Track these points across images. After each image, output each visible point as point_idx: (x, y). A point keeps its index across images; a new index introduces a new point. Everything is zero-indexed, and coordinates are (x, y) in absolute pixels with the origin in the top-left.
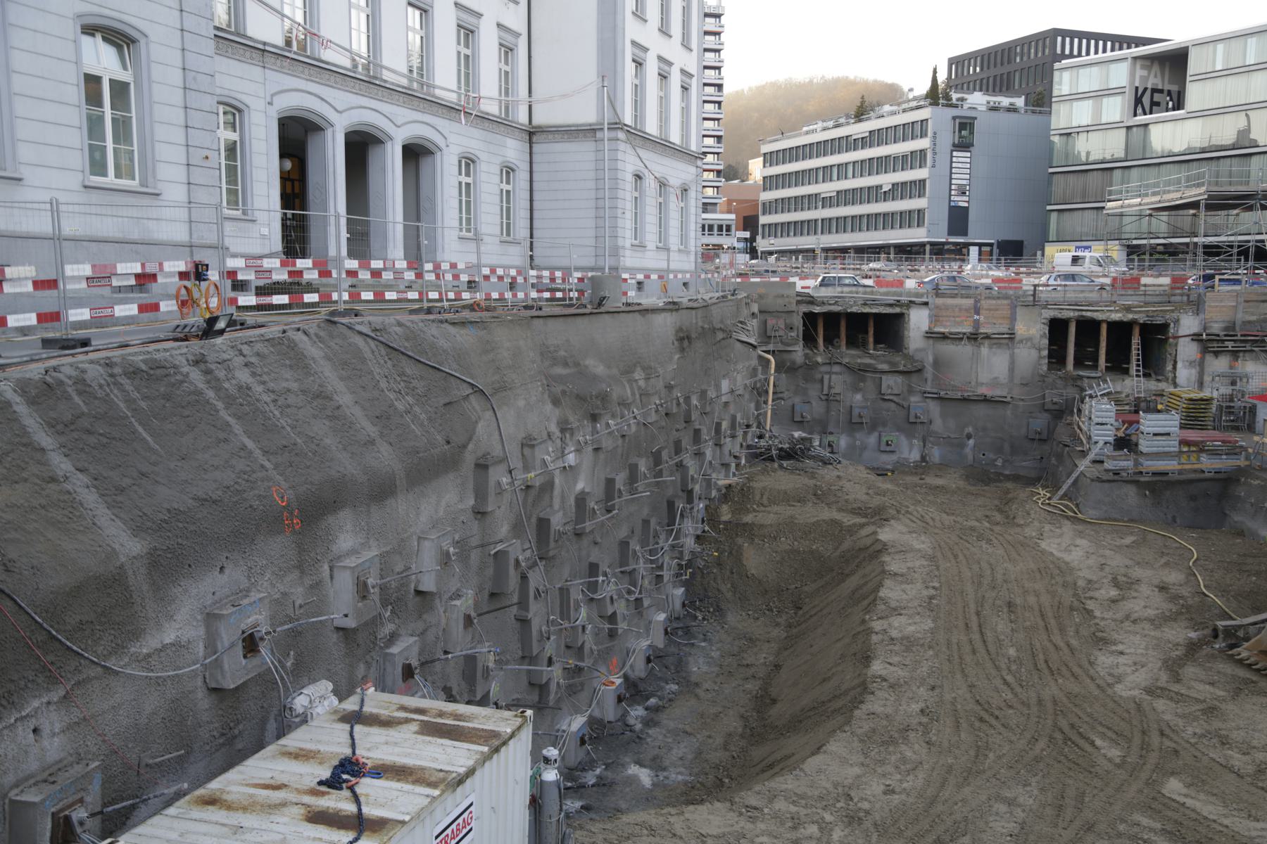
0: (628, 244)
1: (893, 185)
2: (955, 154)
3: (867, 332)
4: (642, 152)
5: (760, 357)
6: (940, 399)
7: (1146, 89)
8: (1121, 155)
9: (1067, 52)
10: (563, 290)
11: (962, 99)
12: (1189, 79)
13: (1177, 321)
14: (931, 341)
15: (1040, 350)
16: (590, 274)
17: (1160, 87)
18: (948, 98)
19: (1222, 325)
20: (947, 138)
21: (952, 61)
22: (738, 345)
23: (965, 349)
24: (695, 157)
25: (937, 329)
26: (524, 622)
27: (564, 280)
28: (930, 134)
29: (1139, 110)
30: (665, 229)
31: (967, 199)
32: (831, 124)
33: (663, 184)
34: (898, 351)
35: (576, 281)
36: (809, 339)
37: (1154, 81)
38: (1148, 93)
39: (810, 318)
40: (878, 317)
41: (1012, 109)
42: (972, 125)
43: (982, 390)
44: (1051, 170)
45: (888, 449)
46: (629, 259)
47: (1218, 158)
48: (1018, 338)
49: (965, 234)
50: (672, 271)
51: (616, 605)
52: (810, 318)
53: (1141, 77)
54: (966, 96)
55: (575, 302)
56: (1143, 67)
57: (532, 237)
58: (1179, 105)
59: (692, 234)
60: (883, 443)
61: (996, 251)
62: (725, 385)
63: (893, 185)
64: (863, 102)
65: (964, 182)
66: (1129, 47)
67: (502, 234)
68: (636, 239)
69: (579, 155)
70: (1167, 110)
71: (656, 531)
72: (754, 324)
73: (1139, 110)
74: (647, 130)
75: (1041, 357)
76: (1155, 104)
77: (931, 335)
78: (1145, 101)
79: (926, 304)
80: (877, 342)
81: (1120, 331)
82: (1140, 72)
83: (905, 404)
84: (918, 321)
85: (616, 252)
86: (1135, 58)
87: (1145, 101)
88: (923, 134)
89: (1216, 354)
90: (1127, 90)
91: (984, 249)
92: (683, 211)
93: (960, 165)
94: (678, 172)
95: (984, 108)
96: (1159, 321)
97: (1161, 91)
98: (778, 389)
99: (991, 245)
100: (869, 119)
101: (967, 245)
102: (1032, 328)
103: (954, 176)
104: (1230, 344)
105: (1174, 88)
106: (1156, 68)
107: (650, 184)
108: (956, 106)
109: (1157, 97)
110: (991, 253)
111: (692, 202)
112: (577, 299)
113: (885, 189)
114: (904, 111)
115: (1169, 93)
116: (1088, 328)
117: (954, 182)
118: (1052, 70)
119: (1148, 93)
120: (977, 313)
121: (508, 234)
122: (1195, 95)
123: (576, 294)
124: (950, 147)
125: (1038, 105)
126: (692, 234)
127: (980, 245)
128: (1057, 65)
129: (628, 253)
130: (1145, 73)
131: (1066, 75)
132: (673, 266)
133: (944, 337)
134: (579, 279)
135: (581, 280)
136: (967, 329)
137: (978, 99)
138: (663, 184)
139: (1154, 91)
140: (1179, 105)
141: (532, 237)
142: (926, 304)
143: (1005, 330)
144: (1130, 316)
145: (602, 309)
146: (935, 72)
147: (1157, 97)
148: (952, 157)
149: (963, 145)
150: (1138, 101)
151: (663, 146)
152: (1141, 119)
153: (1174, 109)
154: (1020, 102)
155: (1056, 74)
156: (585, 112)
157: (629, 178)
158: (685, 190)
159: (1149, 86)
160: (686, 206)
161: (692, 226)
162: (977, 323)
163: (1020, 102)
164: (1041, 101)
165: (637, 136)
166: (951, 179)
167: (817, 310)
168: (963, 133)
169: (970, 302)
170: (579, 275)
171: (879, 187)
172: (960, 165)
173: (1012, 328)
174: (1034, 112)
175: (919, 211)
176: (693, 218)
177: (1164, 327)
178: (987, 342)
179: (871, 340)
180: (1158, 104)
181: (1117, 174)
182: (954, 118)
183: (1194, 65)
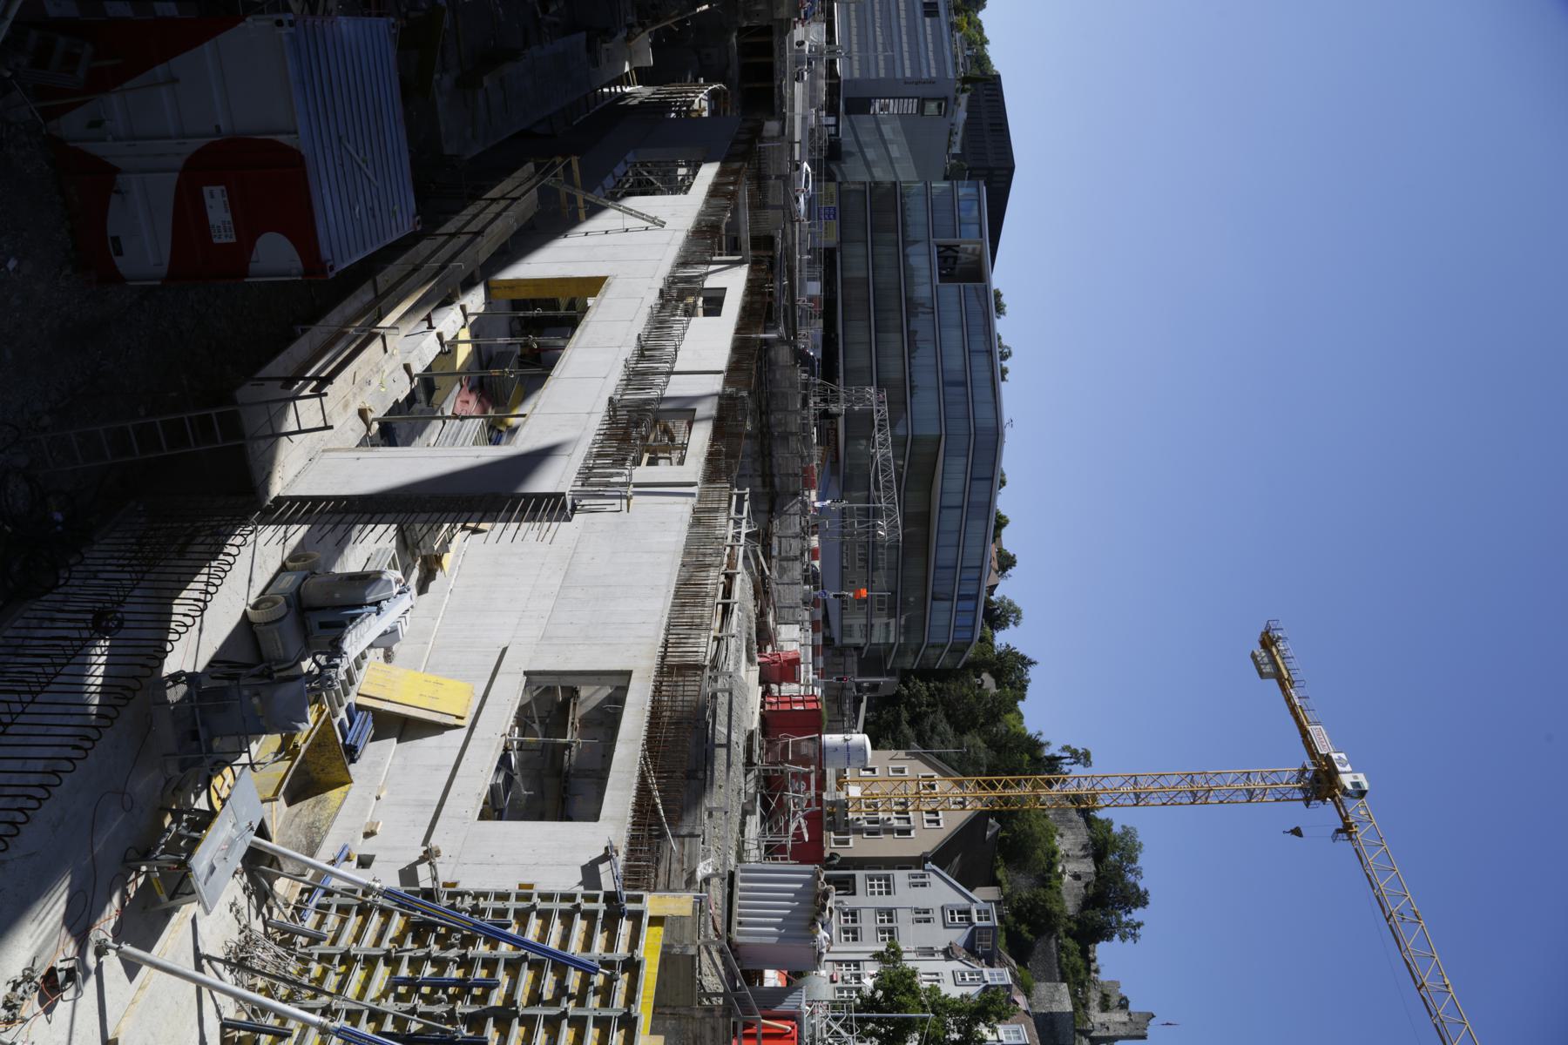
2: (916, 100)
7: (957, 252)
12: (962, 285)
17: (958, 262)
18: (963, 91)
31: (877, 110)
39: (767, 31)
41: (950, 145)
49: (848, 112)
52: (767, 31)
53: (967, 249)
65: (891, 109)
70: (939, 268)
73: (942, 249)
93: (906, 105)
97: (955, 263)
103: (896, 101)
105: (957, 271)
106: (976, 258)
109: (951, 261)
117: (892, 101)
122: (950, 290)
127: (837, 125)
128: (982, 183)
139: (956, 258)
140: (943, 278)
147: (951, 260)
148: (913, 98)
150: (949, 247)
153: (940, 274)
159: (960, 255)
163: (956, 149)
166: (894, 98)
167: (776, 39)
172: (906, 105)
180: (945, 261)
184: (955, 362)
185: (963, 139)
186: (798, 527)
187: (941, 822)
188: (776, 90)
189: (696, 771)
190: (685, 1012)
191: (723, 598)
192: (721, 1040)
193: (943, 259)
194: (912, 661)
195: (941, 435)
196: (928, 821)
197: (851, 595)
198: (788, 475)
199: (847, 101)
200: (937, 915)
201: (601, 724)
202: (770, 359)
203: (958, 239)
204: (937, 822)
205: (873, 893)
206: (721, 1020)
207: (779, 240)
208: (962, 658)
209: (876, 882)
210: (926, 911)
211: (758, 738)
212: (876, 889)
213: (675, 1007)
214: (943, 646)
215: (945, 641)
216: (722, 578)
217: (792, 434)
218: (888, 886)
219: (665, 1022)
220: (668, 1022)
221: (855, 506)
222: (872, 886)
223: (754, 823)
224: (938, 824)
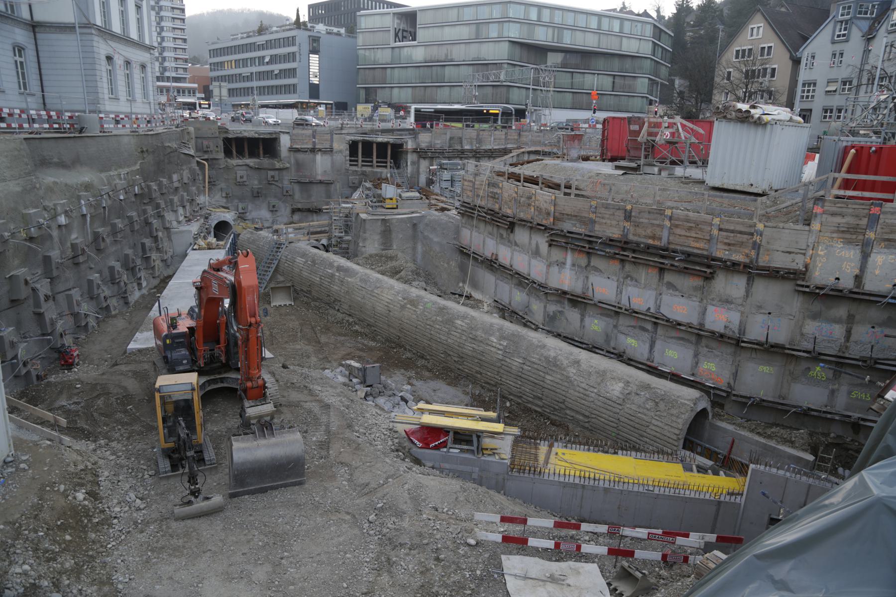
0: (106, 96)
1: (280, 70)
2: (311, 55)
3: (259, 148)
4: (110, 43)
5: (198, 162)
6: (299, 182)
7: (399, 29)
8: (389, 60)
9: (362, 6)
10: (59, 124)
11: (313, 27)
12: (418, 26)
13: (407, 143)
14: (292, 153)
15: (345, 157)
16: (77, 114)
19: (427, 144)
20: (306, 47)
21: (310, 6)
22: (182, 156)
23: (307, 157)
24: (149, 48)
25: (294, 146)
26: (40, 316)
27: (58, 117)
28: (297, 44)
29: (397, 40)
30: (132, 89)
32: (245, 35)
33: (128, 63)
34: (276, 158)
35: (67, 118)
36: (228, 153)
37: (402, 26)
38: (401, 32)
39: (228, 142)
40: (264, 139)
41: (339, 34)
42: (318, 41)
43: (319, 178)
44: (358, 67)
45: (275, 209)
46: (109, 106)
47: (432, 66)
48: (335, 151)
49: (318, 98)
50: (134, 114)
51: (108, 301)
52: (228, 142)
54: (315, 25)
55: (67, 130)
56: (398, 18)
57: (43, 91)
58: (414, 39)
59: (151, 93)
60: (271, 207)
61: (334, 107)
62: (175, 177)
63: (280, 70)
64: (261, 25)
66: (391, 8)
67: (20, 89)
68: (112, 94)
69: (68, 43)
71: (133, 259)
72: (192, 144)
73: (397, 40)
74: (114, 30)
75: (346, 160)
76: (404, 37)
77: (292, 150)
78: (401, 35)
79: (288, 133)
80: (265, 153)
81: (382, 146)
82: (396, 21)
83: (280, 185)
84: (285, 141)
85: (96, 101)
86: (394, 14)
87: (401, 35)
88: (294, 44)
89: (424, 158)
90: (391, 29)
91: (328, 106)
92: (144, 80)
94: (138, 56)
95: (324, 32)
96: (399, 142)
97: (406, 31)
98: (212, 180)
99: (331, 104)
100: (265, 34)
101: (320, 104)
102: (341, 146)
104: (430, 154)
107: (119, 61)
108: (310, 30)
109: (405, 34)
110: (332, 108)
111: (150, 74)
112: (69, 129)
113: (276, 72)
114: (284, 31)
115: (410, 33)
116: (367, 145)
118: (355, 16)
119: (401, 32)
120: (314, 137)
121: (25, 88)
122: (421, 34)
123: (68, 126)
124: (308, 52)
125: (352, 33)
126: (151, 93)
128: (358, 13)
129: (107, 103)
130: (399, 21)
131: (363, 19)
132: (134, 110)
133: (298, 150)
134: (69, 117)
135: (71, 117)
136: (310, 146)
137: (321, 27)
138: (128, 63)
139: (404, 31)
140: (414, 39)
141: (43, 91)
142: (288, 133)
143: (328, 147)
144: (386, 140)
145: (83, 135)
146: (298, 11)
147: (405, 34)
149: (315, 51)
150: (396, 35)
151: (124, 39)
152: (398, 44)
154: (343, 31)
155: (358, 18)
156: (68, 15)
157: (104, 58)
158: (143, 67)
160: (146, 76)
161: (151, 88)
162: (314, 143)
163: (343, 31)
164: (352, 31)
165: (106, 33)
167: (230, 136)
168: (314, 45)
169: (310, 132)
170: (69, 114)
171: (272, 71)
173: (331, 146)
174: (349, 36)
175: (294, 85)
176: (150, 84)
177: (401, 146)
178: (320, 153)
179: (261, 152)
181: (389, 71)
182: (309, 37)
183: (420, 19)
184: (464, 32)
185: (335, 26)
186: (540, 134)
187: (769, 45)
188: (262, 137)
189: (626, 210)
190: (814, 237)
191: (519, 181)
192: (844, 210)
193: (404, 38)
194: (664, 68)
195: (510, 41)
196: (769, 54)
197: (594, 101)
198: (506, 139)
199: (311, 97)
200: (838, 48)
201: (587, 277)
202: (427, 146)
203: (391, 29)
204: (770, 48)
205: (813, 96)
206: (826, 208)
207: (353, 138)
208: (666, 33)
209: (805, 94)
210: (834, 55)
211: (622, 163)
212: (810, 94)
213: (808, 246)
214: (654, 44)
215: (651, 43)
216: (510, 181)
217: (478, 135)
218: (809, 85)
219: (819, 255)
220: (820, 253)
221: (531, 95)
222: (807, 97)
223: (679, 171)
224: (771, 47)
